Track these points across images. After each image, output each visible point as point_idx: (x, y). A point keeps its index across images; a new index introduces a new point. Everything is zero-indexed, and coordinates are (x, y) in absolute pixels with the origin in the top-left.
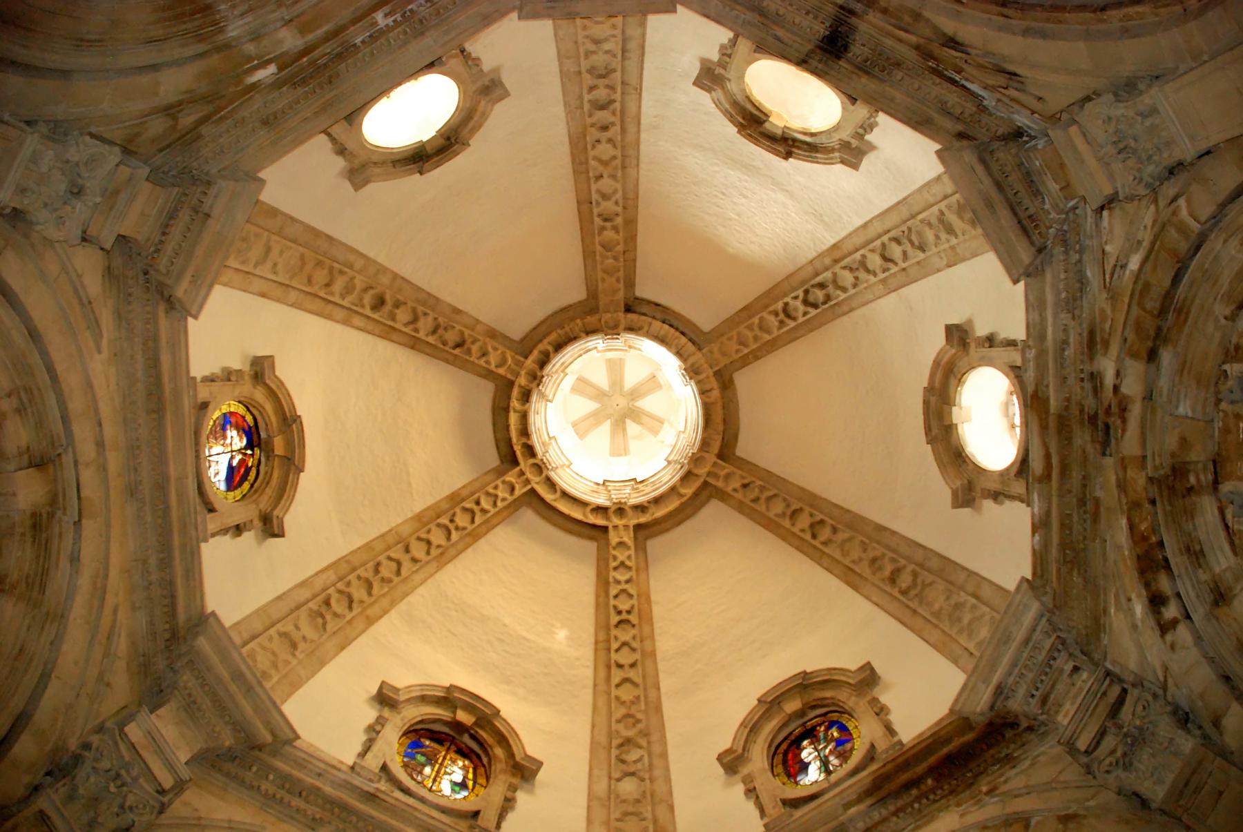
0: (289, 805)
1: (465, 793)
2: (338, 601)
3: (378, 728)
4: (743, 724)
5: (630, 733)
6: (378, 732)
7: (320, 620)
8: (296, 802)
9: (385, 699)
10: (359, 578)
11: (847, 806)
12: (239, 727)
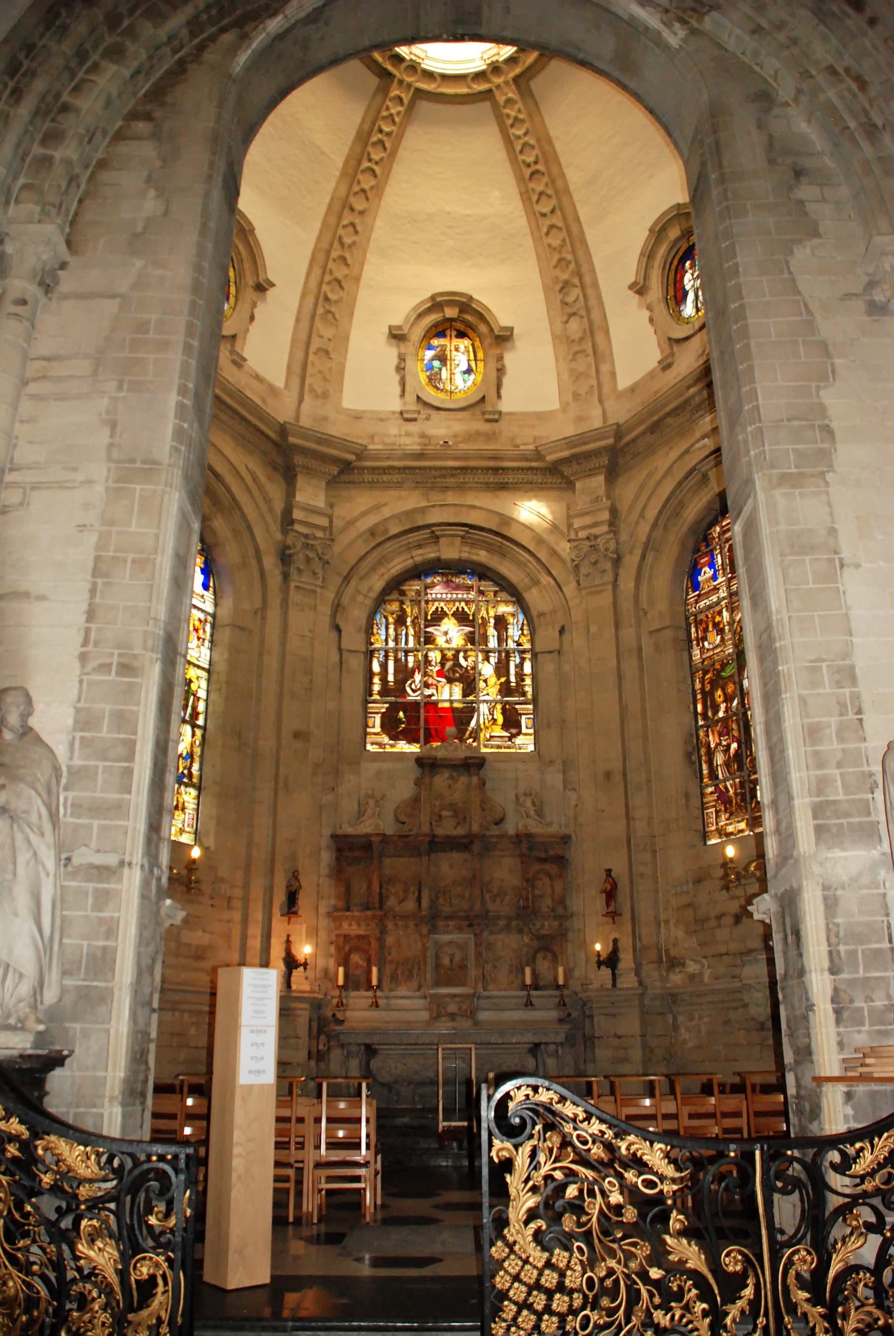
1: (473, 377)
2: (332, 291)
4: (642, 254)
5: (565, 276)
8: (385, 478)
9: (397, 336)
10: (334, 260)
11: (689, 387)
12: (335, 460)
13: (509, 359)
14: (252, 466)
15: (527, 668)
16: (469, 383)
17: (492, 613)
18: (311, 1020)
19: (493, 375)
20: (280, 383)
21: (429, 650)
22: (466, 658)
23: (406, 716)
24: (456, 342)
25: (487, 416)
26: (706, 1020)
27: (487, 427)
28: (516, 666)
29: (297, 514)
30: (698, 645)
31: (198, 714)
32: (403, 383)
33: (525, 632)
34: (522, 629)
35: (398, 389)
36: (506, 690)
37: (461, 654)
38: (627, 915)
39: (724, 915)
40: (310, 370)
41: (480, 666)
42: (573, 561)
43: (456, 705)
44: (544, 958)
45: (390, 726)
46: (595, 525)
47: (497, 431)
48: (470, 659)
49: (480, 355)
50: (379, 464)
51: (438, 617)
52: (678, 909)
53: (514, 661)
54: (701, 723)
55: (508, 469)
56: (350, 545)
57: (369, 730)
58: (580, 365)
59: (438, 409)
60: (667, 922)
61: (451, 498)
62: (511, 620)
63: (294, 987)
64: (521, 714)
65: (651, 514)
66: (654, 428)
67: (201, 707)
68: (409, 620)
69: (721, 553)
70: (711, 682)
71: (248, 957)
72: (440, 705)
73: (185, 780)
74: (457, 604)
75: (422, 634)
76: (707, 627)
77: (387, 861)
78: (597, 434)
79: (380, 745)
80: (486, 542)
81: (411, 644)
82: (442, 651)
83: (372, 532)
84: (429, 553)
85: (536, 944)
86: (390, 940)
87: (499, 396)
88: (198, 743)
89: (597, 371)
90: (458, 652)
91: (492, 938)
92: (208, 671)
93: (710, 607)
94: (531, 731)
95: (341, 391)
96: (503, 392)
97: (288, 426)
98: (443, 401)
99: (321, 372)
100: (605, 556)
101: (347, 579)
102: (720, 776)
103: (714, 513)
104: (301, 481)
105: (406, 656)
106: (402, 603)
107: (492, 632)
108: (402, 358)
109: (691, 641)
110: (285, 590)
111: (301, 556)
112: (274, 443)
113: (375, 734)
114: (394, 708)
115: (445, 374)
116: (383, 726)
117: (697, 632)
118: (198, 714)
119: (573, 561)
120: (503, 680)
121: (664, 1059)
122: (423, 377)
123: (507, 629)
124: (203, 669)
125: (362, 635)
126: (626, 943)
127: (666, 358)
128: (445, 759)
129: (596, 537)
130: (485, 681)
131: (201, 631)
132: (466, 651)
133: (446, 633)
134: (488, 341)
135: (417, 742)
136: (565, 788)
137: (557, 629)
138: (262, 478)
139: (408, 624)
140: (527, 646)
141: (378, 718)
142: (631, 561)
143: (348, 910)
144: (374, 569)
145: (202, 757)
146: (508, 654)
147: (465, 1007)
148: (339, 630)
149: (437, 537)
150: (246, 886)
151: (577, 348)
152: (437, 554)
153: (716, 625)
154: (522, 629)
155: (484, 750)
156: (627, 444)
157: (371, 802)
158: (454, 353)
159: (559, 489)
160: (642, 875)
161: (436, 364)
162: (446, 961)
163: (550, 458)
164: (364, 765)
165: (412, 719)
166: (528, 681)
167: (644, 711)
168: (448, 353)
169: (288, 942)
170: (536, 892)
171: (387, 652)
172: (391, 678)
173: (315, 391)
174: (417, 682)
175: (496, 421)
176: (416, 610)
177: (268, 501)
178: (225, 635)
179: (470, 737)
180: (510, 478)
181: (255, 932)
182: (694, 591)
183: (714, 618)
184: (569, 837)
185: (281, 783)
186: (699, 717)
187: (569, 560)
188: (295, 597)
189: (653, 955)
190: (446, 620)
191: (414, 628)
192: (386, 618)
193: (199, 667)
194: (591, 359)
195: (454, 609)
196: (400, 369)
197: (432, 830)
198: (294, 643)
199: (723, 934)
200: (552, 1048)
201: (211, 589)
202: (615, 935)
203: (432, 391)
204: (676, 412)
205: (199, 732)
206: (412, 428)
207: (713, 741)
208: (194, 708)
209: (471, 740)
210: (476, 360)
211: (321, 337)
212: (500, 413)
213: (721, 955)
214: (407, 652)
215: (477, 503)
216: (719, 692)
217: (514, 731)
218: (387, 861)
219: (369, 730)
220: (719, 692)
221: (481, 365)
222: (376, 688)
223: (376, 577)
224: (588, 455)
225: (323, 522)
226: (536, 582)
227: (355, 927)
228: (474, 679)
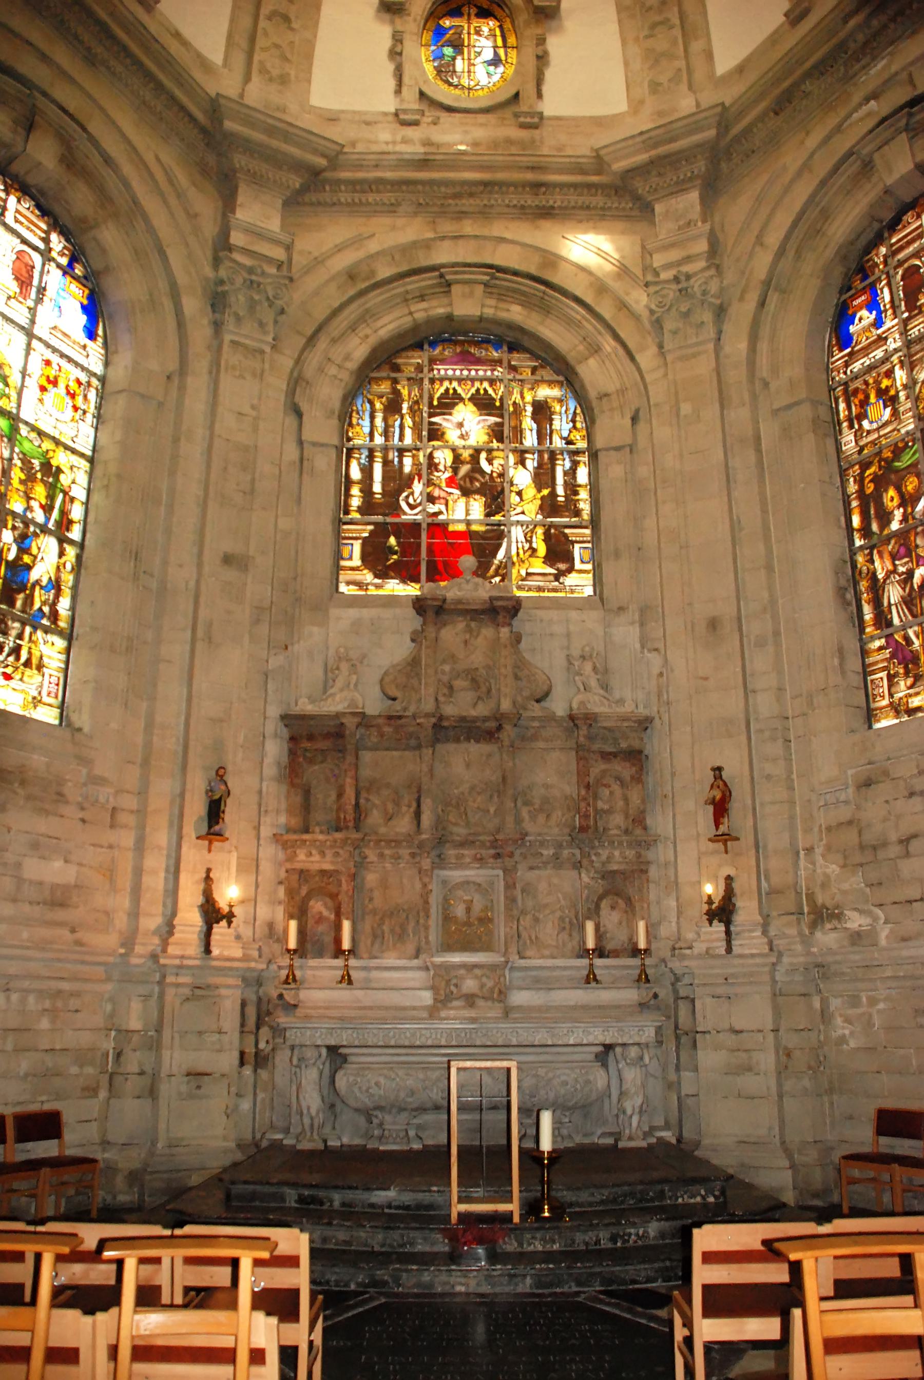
0: (369, 204)
1: (501, 69)
3: (398, 49)
6: (400, 54)
8: (371, 198)
13: (554, 44)
14: (165, 158)
15: (582, 476)
16: (496, 78)
17: (529, 397)
18: (244, 1004)
19: (531, 63)
21: (434, 448)
22: (490, 461)
23: (399, 544)
24: (476, 23)
25: (522, 119)
26: (881, 1006)
28: (565, 473)
29: (237, 238)
30: (851, 426)
31: (71, 522)
33: (579, 425)
34: (574, 421)
35: (392, 84)
36: (550, 506)
37: (483, 455)
38: (747, 839)
40: (261, 42)
41: (512, 472)
43: (475, 528)
44: (613, 908)
46: (688, 259)
47: (537, 138)
48: (496, 463)
49: (512, 40)
50: (360, 175)
51: (448, 403)
52: (829, 829)
54: (858, 542)
55: (555, 185)
56: (317, 293)
57: (343, 563)
58: (661, 43)
59: (450, 109)
60: (809, 850)
61: (468, 227)
62: (557, 407)
63: (216, 952)
64: (573, 542)
65: (774, 239)
67: (77, 512)
68: (405, 406)
69: (889, 284)
70: (875, 479)
71: (142, 904)
72: (451, 528)
73: (45, 622)
74: (477, 384)
75: (425, 426)
76: (867, 397)
78: (693, 125)
79: (360, 585)
80: (523, 294)
81: (408, 440)
82: (454, 450)
83: (351, 275)
86: (371, 878)
87: (540, 95)
88: (69, 567)
89: (686, 51)
90: (478, 451)
91: (531, 876)
92: (91, 461)
93: (871, 368)
94: (589, 567)
95: (309, 82)
96: (545, 89)
97: (222, 101)
98: (458, 98)
99: (277, 46)
102: (896, 621)
103: (876, 225)
106: (395, 381)
107: (528, 423)
108: (397, 38)
112: (203, 131)
113: (352, 569)
114: (381, 531)
115: (460, 65)
116: (364, 557)
117: (849, 408)
118: (71, 522)
119: (652, 312)
120: (545, 492)
121: (810, 1068)
122: (429, 69)
123: (551, 420)
124: (82, 455)
128: (459, 601)
129: (688, 277)
130: (519, 493)
132: (490, 451)
133: (460, 425)
135: (415, 579)
136: (643, 647)
139: (404, 411)
140: (582, 444)
141: (357, 546)
143: (306, 830)
144: (353, 328)
145: (75, 588)
147: (490, 984)
149: (449, 284)
150: (143, 793)
151: (658, 18)
152: (448, 310)
153: (882, 393)
154: (574, 421)
155: (518, 593)
156: (737, 139)
157: (344, 666)
158: (474, 37)
159: (628, 218)
160: (768, 777)
161: (448, 51)
162: (459, 911)
163: (619, 166)
164: (334, 612)
165: (409, 549)
166: (584, 494)
169: (208, 879)
170: (600, 804)
171: (371, 451)
172: (377, 488)
173: (268, 72)
174: (417, 494)
175: (535, 127)
176: (416, 392)
177: (193, 216)
178: (118, 407)
179: (496, 574)
180: (556, 200)
181: (155, 863)
182: (841, 350)
183: (877, 382)
185: (200, 633)
186: (856, 536)
187: (645, 314)
188: (228, 356)
190: (460, 407)
191: (413, 418)
192: (371, 403)
193: (74, 451)
194: (677, 32)
195: (473, 391)
196: (395, 54)
197: (438, 707)
198: (227, 422)
200: (633, 1052)
201: (100, 340)
202: (731, 872)
206: (410, 132)
207: (880, 568)
208: (64, 513)
209: (498, 579)
210: (505, 46)
212: (541, 115)
213: (910, 902)
214: (401, 451)
215: (508, 235)
216: (892, 492)
217: (562, 566)
218: (367, 757)
219: (343, 563)
220: (892, 492)
221: (513, 54)
222: (356, 502)
225: (279, 253)
226: (595, 350)
227: (316, 857)
228: (503, 491)
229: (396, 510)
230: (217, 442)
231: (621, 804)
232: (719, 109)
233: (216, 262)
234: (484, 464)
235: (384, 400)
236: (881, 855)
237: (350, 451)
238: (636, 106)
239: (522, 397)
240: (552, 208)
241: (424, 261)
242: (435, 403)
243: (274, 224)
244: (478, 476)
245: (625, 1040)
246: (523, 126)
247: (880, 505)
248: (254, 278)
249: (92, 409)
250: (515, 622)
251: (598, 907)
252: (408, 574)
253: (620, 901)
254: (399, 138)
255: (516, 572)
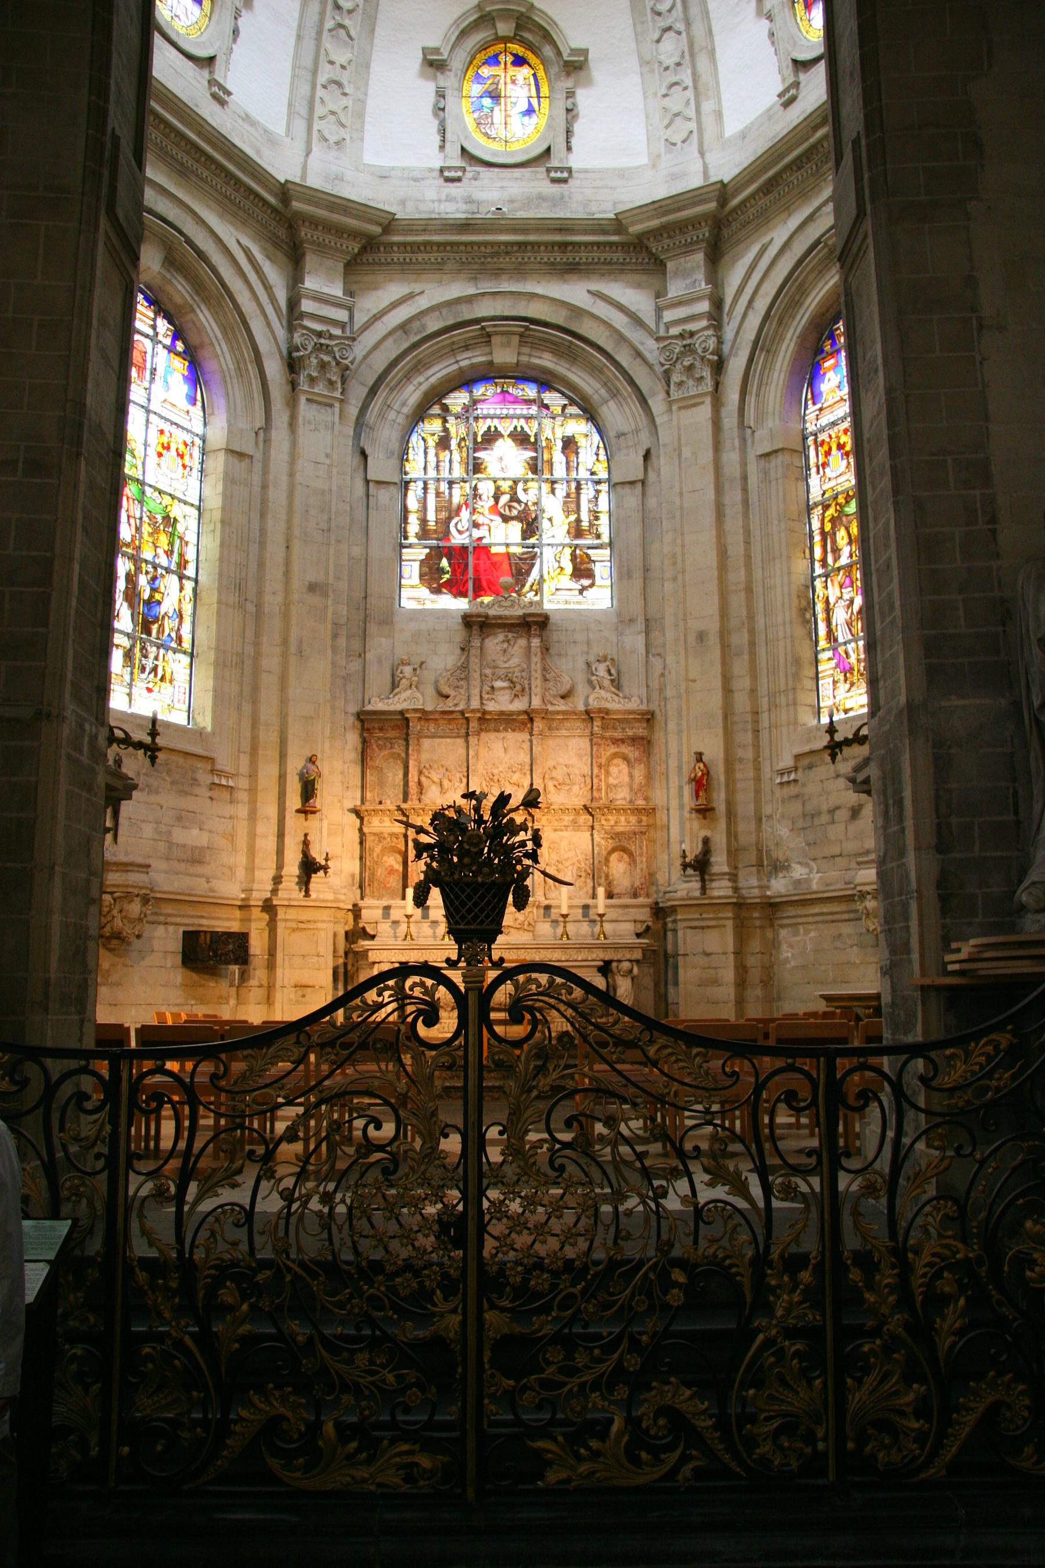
0: (418, 263)
1: (534, 119)
6: (443, 109)
7: (342, 32)
8: (421, 257)
11: (815, 129)
12: (354, 234)
13: (584, 98)
15: (603, 504)
16: (530, 129)
17: (559, 434)
18: (335, 935)
20: (279, 129)
22: (525, 490)
23: (450, 565)
24: (513, 70)
25: (553, 174)
27: (556, 189)
28: (590, 501)
29: (307, 306)
30: (818, 472)
31: (186, 562)
32: (443, 132)
35: (437, 139)
36: (577, 532)
37: (520, 486)
38: (721, 807)
39: (838, 808)
40: (319, 111)
42: (663, 365)
43: (513, 550)
45: (431, 575)
47: (566, 194)
49: (545, 90)
50: (410, 239)
51: (491, 437)
53: (587, 493)
55: (579, 244)
58: (676, 102)
61: (506, 286)
62: (582, 441)
65: (762, 304)
66: (768, 188)
67: (190, 554)
68: (454, 443)
70: (833, 520)
72: (493, 550)
76: (830, 449)
77: (426, 743)
78: (694, 197)
81: (458, 472)
84: (476, 357)
85: (611, 844)
87: (569, 149)
90: (516, 482)
92: (199, 509)
93: (834, 424)
94: (608, 582)
95: (362, 140)
96: (574, 141)
97: (289, 186)
98: (495, 153)
99: (333, 113)
100: (702, 358)
101: (373, 391)
104: (310, 260)
105: (450, 488)
106: (445, 421)
107: (559, 458)
108: (441, 94)
109: (808, 468)
110: (292, 404)
111: (314, 361)
112: (274, 210)
114: (436, 553)
115: (498, 116)
116: (422, 576)
118: (186, 562)
120: (573, 518)
121: (762, 981)
122: (469, 121)
123: (577, 453)
125: (395, 462)
126: (720, 840)
127: (787, 90)
128: (500, 617)
129: (692, 334)
130: (550, 520)
131: (187, 458)
134: (555, 69)
135: (464, 595)
136: (647, 652)
137: (643, 453)
138: (259, 257)
142: (736, 366)
144: (408, 377)
146: (578, 488)
148: (364, 455)
149: (489, 335)
150: (253, 776)
151: (674, 79)
154: (597, 455)
155: (547, 606)
156: (735, 210)
157: (408, 670)
158: (510, 86)
159: (645, 271)
160: (741, 760)
161: (487, 102)
163: (635, 229)
167: (748, 557)
168: (501, 86)
169: (306, 843)
170: (611, 781)
171: (425, 483)
172: (431, 516)
173: (326, 140)
175: (564, 181)
178: (217, 464)
180: (583, 256)
181: (267, 830)
183: (838, 437)
184: (653, 714)
185: (293, 649)
188: (306, 411)
189: (752, 858)
190: (500, 442)
193: (185, 503)
194: (690, 94)
196: (439, 110)
198: (306, 471)
199: (836, 831)
201: (199, 404)
203: (482, 140)
204: (797, 164)
205: (189, 585)
206: (453, 189)
207: (833, 592)
208: (181, 555)
210: (539, 97)
211: (332, 63)
212: (570, 170)
213: (833, 857)
215: (539, 290)
217: (586, 582)
221: (545, 103)
222: (413, 527)
223: (411, 388)
224: (682, 227)
225: (342, 315)
228: (536, 517)
229: (446, 535)
230: (299, 491)
231: (627, 779)
232: (718, 186)
233: (291, 329)
234: (521, 495)
235: (436, 437)
236: (816, 821)
237: (407, 483)
238: (654, 163)
239: (553, 433)
240: (578, 264)
241: (468, 313)
242: (479, 439)
243: (336, 290)
244: (515, 504)
245: (619, 957)
246: (555, 181)
247: (834, 542)
248: (323, 341)
249: (197, 466)
250: (544, 634)
251: (607, 860)
252: (457, 588)
253: (625, 856)
254: (444, 197)
255: (548, 588)
